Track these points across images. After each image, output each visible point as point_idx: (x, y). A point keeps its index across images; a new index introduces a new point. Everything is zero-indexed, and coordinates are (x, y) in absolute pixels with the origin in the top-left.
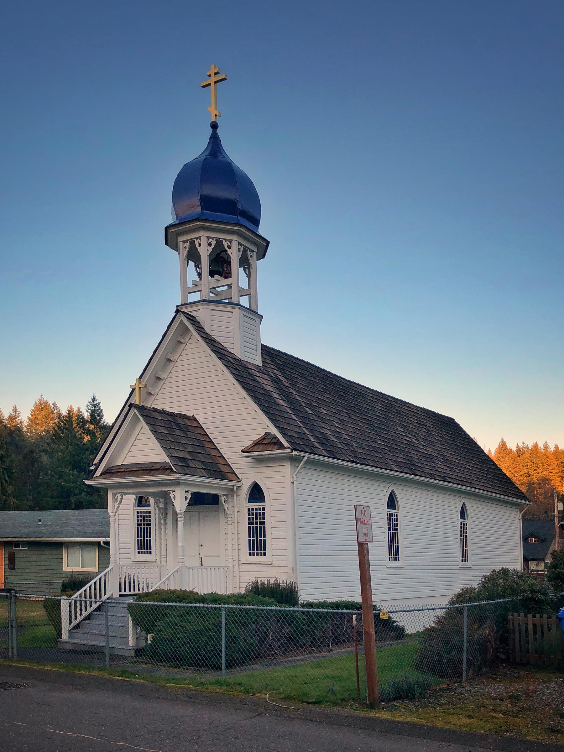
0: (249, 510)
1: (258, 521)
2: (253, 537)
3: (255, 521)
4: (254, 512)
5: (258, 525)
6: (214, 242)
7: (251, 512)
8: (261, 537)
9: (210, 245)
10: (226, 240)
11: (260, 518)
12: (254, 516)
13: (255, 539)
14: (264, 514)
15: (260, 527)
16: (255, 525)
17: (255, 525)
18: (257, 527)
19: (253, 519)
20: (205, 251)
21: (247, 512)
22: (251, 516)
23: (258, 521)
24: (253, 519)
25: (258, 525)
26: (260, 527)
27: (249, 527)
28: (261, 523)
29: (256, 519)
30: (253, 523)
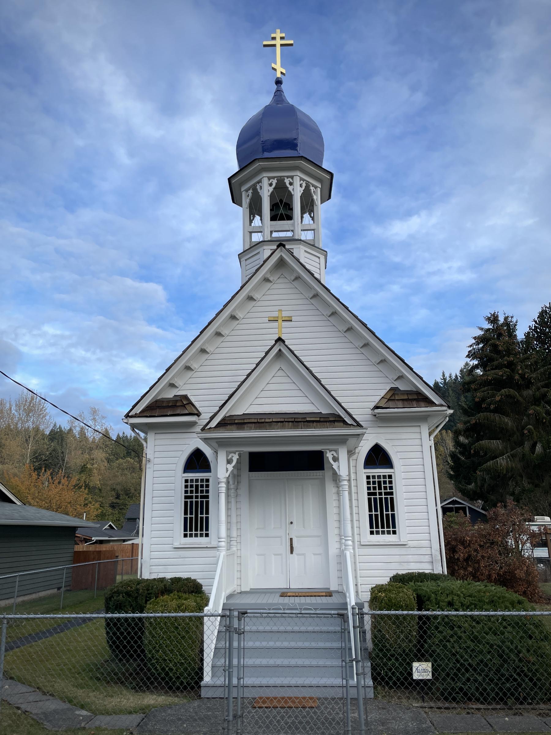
0: (368, 477)
1: (383, 491)
2: (376, 510)
3: (377, 491)
4: (377, 480)
5: (383, 496)
6: (274, 182)
7: (371, 480)
8: (387, 510)
9: (271, 185)
10: (288, 177)
11: (385, 488)
12: (377, 485)
13: (379, 513)
14: (391, 482)
15: (386, 499)
16: (378, 496)
17: (378, 496)
18: (381, 499)
19: (374, 488)
20: (266, 192)
21: (365, 480)
22: (372, 486)
23: (383, 491)
24: (374, 488)
25: (383, 496)
26: (386, 499)
27: (368, 498)
28: (386, 494)
29: (380, 488)
30: (375, 494)
